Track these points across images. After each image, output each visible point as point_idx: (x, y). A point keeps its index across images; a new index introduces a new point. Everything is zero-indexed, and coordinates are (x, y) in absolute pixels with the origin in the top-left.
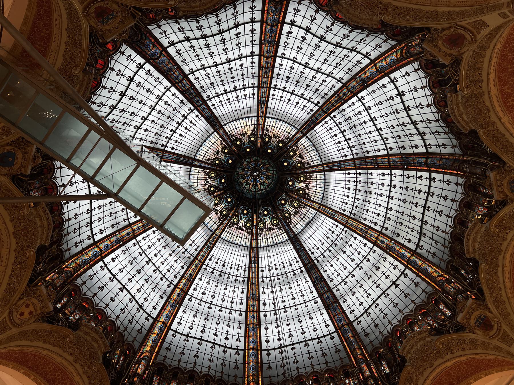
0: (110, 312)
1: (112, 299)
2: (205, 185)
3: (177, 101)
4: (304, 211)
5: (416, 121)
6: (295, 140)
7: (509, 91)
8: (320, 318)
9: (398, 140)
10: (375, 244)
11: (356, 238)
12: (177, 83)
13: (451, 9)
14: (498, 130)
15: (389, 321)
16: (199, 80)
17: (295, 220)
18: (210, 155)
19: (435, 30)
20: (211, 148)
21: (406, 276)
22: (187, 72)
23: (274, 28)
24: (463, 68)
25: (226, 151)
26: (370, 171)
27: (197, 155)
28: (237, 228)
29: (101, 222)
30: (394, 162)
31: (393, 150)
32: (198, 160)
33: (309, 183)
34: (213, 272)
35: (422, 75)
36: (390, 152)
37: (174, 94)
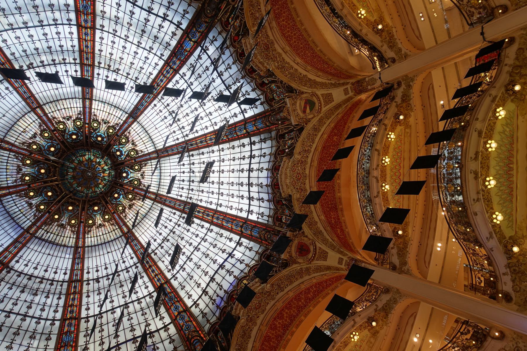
2: (64, 118)
3: (150, 69)
4: (68, 232)
5: (214, 279)
7: (285, 315)
9: (188, 280)
11: (59, 298)
13: (323, 231)
14: (251, 330)
17: (55, 228)
18: (101, 116)
19: (303, 233)
22: (181, 72)
24: (285, 272)
27: (97, 102)
28: (18, 166)
30: (165, 289)
31: (176, 281)
32: (91, 104)
33: (104, 225)
36: (172, 281)
37: (157, 64)
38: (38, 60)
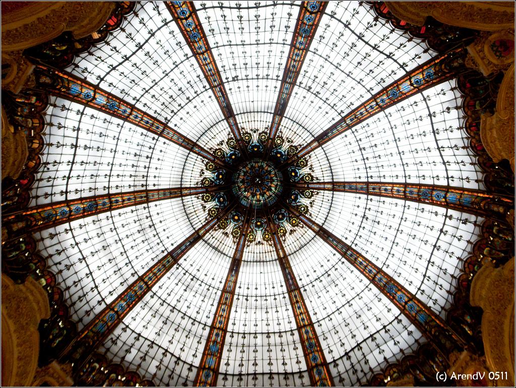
0: (60, 280)
1: (68, 267)
4: (299, 231)
6: (308, 148)
8: (293, 353)
10: (373, 281)
12: (199, 54)
15: (370, 368)
16: (223, 58)
20: (219, 138)
21: (400, 321)
23: (313, 15)
25: (232, 144)
26: (383, 199)
29: (80, 181)
34: (185, 274)
35: (458, 94)
38: (143, 169)
